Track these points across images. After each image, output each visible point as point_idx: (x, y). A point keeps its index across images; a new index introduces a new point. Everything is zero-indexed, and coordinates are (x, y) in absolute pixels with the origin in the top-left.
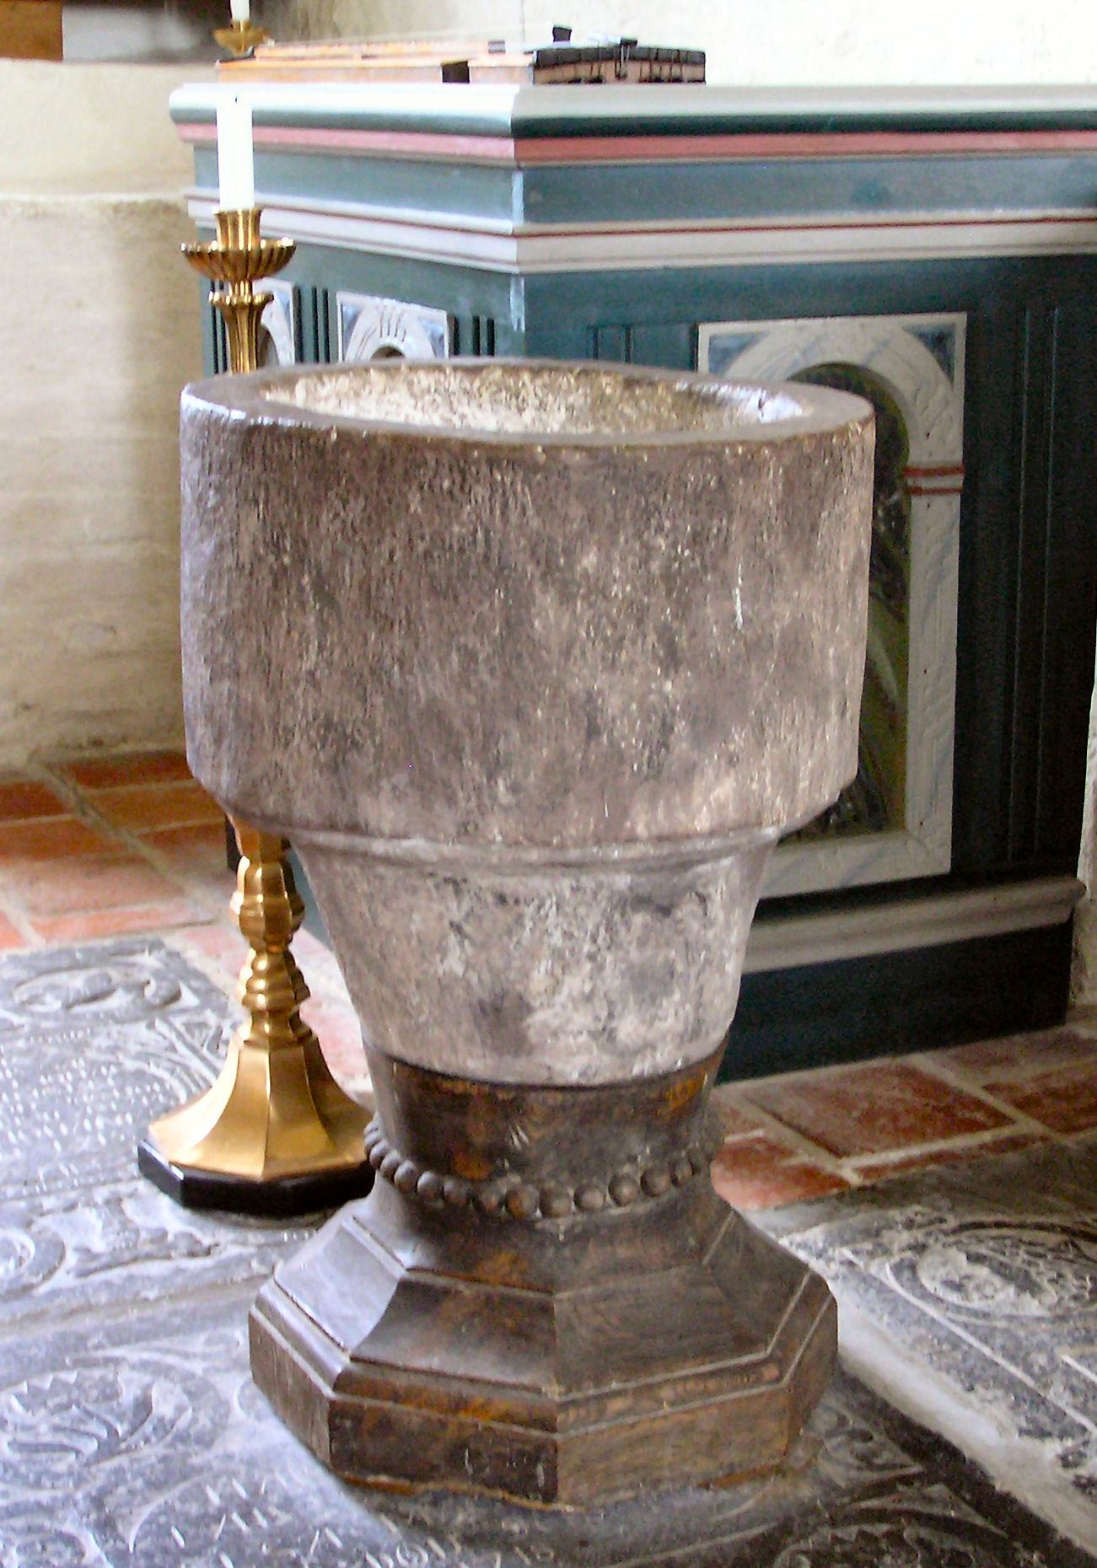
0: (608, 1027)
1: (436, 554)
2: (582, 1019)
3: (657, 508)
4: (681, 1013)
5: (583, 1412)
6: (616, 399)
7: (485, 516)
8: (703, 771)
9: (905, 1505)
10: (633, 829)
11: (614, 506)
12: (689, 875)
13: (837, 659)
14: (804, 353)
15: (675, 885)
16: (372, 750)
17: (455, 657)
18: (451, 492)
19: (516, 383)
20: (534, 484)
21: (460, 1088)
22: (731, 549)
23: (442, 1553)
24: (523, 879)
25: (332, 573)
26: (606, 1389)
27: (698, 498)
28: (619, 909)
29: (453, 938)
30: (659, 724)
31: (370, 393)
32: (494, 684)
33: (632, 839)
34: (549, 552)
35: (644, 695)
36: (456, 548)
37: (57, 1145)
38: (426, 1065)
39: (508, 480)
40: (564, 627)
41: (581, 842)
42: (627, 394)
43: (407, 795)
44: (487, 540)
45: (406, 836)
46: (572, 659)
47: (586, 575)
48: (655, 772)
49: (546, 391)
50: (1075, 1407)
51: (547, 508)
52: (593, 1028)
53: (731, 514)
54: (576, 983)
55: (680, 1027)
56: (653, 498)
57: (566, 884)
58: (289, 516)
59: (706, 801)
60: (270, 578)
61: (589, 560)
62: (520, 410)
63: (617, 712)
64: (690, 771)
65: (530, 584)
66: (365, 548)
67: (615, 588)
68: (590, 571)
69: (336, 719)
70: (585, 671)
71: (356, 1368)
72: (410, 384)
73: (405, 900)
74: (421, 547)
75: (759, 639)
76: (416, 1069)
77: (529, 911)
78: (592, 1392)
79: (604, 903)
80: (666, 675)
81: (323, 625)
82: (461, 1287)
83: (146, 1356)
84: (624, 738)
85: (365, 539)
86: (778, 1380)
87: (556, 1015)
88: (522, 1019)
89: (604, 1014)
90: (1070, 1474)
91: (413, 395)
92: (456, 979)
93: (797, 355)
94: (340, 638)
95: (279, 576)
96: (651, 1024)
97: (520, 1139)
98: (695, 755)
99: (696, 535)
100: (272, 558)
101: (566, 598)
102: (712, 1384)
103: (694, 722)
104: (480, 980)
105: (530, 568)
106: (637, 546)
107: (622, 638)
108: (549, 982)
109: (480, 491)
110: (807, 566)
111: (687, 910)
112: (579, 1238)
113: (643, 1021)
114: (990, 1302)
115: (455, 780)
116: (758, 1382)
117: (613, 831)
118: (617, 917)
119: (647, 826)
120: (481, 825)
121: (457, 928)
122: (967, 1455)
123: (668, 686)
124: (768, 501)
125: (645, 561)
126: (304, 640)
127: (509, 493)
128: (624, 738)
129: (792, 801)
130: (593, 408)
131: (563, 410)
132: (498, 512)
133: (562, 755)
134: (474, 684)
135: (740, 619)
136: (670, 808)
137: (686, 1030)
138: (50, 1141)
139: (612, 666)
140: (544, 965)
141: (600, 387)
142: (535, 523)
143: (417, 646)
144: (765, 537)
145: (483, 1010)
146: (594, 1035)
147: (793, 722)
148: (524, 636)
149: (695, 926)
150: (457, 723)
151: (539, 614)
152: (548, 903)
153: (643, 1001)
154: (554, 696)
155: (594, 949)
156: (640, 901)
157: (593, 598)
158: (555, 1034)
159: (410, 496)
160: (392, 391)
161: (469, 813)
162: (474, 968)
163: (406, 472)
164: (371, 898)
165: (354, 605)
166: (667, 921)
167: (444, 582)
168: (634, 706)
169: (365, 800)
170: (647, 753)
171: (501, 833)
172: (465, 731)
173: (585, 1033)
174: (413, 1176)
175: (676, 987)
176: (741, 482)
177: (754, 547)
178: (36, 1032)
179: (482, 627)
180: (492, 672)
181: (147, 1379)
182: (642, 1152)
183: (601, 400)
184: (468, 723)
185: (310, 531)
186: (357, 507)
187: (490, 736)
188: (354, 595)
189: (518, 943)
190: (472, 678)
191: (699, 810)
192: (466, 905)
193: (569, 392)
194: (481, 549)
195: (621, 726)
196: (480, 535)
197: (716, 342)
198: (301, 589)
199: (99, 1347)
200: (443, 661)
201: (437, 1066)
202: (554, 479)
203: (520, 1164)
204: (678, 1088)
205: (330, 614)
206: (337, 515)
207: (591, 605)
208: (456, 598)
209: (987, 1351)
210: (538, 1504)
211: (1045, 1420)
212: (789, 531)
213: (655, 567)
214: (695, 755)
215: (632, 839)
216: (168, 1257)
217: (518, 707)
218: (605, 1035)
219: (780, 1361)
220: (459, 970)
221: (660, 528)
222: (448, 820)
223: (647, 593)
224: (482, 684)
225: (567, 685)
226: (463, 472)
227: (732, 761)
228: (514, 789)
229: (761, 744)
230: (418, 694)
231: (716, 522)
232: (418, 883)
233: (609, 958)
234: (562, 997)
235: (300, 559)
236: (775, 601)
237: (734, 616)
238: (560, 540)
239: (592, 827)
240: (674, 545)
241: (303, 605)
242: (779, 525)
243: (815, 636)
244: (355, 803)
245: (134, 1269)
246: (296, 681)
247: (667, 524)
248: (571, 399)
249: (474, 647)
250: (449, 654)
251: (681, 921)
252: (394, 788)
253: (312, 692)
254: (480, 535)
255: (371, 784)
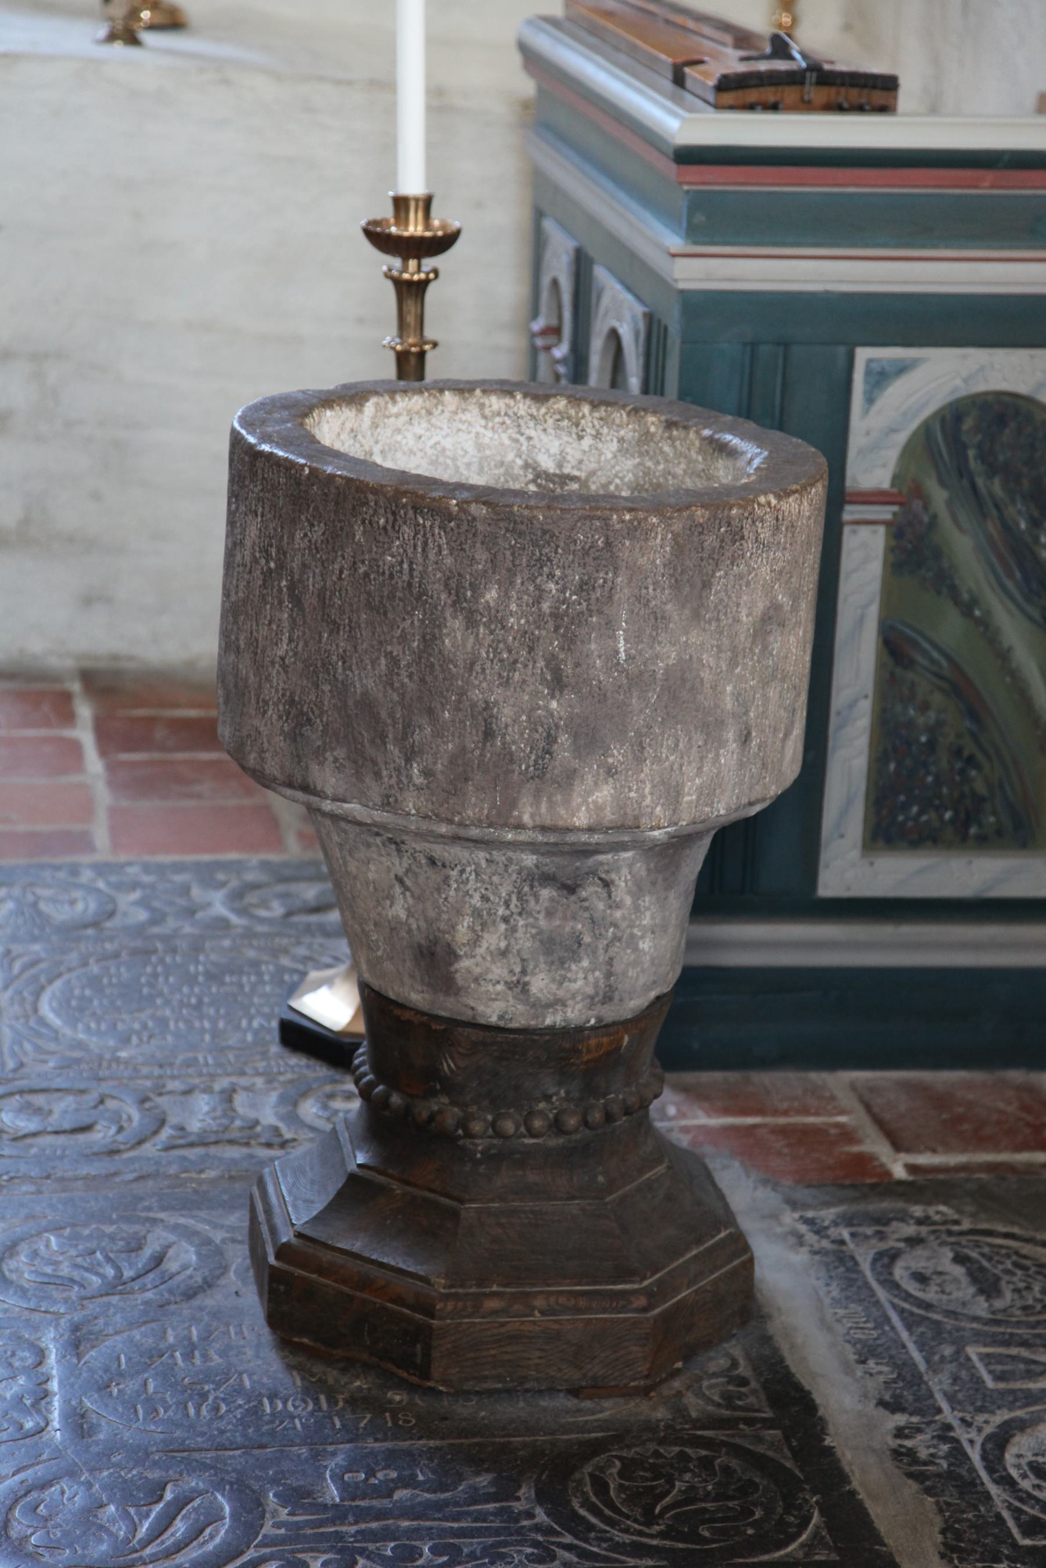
0: (522, 981)
1: (372, 576)
2: (498, 971)
3: (549, 560)
4: (591, 978)
5: (460, 1304)
6: (657, 438)
7: (410, 551)
8: (583, 776)
9: (738, 1441)
10: (520, 817)
11: (513, 554)
12: (591, 861)
13: (737, 696)
14: (966, 381)
15: (577, 868)
16: (321, 728)
17: (383, 661)
18: (385, 528)
19: (577, 413)
20: (448, 530)
21: (407, 1015)
22: (617, 597)
23: (324, 1406)
24: (447, 847)
25: (300, 581)
26: (487, 1290)
27: (586, 553)
28: (528, 883)
29: (398, 889)
30: (544, 734)
31: (443, 411)
32: (411, 686)
33: (519, 826)
34: (459, 587)
35: (533, 710)
36: (387, 573)
37: (207, 1038)
38: (383, 992)
39: (428, 524)
40: (469, 646)
41: (478, 823)
42: (666, 435)
43: (345, 767)
44: (411, 570)
45: (345, 801)
46: (474, 674)
47: (488, 607)
48: (540, 774)
49: (602, 423)
50: (945, 1394)
51: (458, 548)
52: (509, 979)
53: (616, 569)
54: (493, 939)
55: (590, 990)
56: (546, 550)
57: (481, 855)
58: (275, 529)
59: (585, 801)
60: (261, 577)
61: (491, 595)
62: (580, 438)
63: (509, 721)
64: (571, 775)
65: (442, 611)
66: (323, 563)
67: (512, 620)
68: (492, 604)
69: (297, 698)
70: (484, 685)
71: (294, 1241)
72: (482, 406)
73: (362, 853)
74: (362, 569)
75: (641, 673)
76: (378, 994)
77: (454, 874)
78: (473, 1290)
79: (514, 876)
80: (553, 697)
81: (293, 621)
82: (395, 1185)
83: (182, 1221)
84: (514, 742)
85: (324, 557)
86: (645, 1310)
87: (477, 965)
88: (451, 964)
89: (518, 969)
90: (894, 1443)
91: (484, 417)
92: (401, 923)
93: (958, 382)
94: (304, 633)
95: (268, 574)
96: (561, 984)
97: (449, 1066)
98: (576, 764)
99: (583, 584)
100: (263, 561)
101: (471, 623)
102: (582, 1303)
103: (576, 736)
104: (419, 928)
105: (443, 596)
106: (531, 588)
107: (515, 662)
108: (471, 935)
109: (407, 531)
110: (696, 615)
111: (591, 890)
112: (495, 1159)
113: (553, 980)
114: (945, 1297)
115: (380, 760)
116: (623, 1309)
117: (503, 817)
118: (526, 889)
119: (532, 816)
120: (400, 799)
121: (400, 880)
122: (821, 1412)
123: (554, 704)
124: (654, 561)
125: (537, 601)
126: (279, 632)
127: (428, 535)
128: (514, 742)
129: (674, 811)
130: (639, 442)
131: (615, 440)
132: (420, 550)
133: (463, 750)
134: (396, 685)
135: (623, 656)
136: (552, 805)
137: (597, 994)
138: (203, 1030)
139: (506, 683)
140: (467, 921)
141: (645, 424)
142: (449, 561)
143: (355, 648)
144: (651, 590)
145: (421, 952)
146: (510, 986)
147: (677, 745)
148: (437, 650)
149: (601, 906)
150: (384, 714)
151: (449, 635)
152: (468, 869)
153: (552, 963)
154: (459, 701)
155: (508, 913)
156: (548, 879)
157: (493, 627)
158: (476, 980)
159: (356, 527)
160: (464, 411)
161: (391, 787)
162: (413, 916)
163: (354, 508)
164: (341, 846)
165: (315, 609)
166: (573, 898)
167: (377, 599)
168: (524, 718)
169: (314, 767)
170: (533, 757)
171: (414, 807)
172: (389, 721)
173: (502, 983)
174: (371, 1085)
175: (582, 954)
176: (627, 543)
177: (638, 599)
178: (249, 934)
179: (403, 639)
180: (410, 676)
181: (172, 1238)
182: (557, 1094)
183: (646, 437)
184: (392, 715)
185: (288, 543)
186: (319, 530)
187: (408, 728)
188: (315, 601)
189: (446, 899)
190: (395, 678)
191: (578, 810)
192: (406, 862)
193: (620, 426)
194: (406, 578)
195: (513, 733)
196: (405, 566)
197: (873, 365)
198: (280, 590)
199: (149, 1209)
200: (374, 662)
201: (392, 995)
202: (464, 527)
203: (449, 1087)
204: (593, 1042)
205: (298, 615)
206: (306, 535)
207: (492, 632)
208: (385, 614)
209: (904, 1335)
210: (414, 1379)
211: (908, 1396)
212: (676, 586)
213: (546, 606)
214: (576, 764)
215: (519, 826)
216: (247, 1144)
217: (430, 708)
218: (520, 987)
219: (654, 1296)
220: (403, 915)
221: (551, 576)
222: (375, 792)
223: (538, 628)
224: (403, 685)
225: (469, 694)
226: (394, 513)
227: (611, 772)
228: (427, 773)
229: (640, 760)
230: (355, 687)
231: (602, 575)
232: (371, 840)
233: (521, 923)
234: (480, 951)
235: (281, 566)
236: (660, 643)
237: (617, 652)
238: (468, 577)
239: (486, 812)
240: (563, 591)
241: (281, 602)
242: (666, 582)
243: (705, 675)
244: (307, 767)
245: (213, 1150)
246: (273, 663)
247: (558, 573)
248: (622, 433)
249: (398, 655)
250: (378, 658)
251: (584, 900)
252: (336, 760)
253: (283, 676)
254: (405, 566)
255: (319, 754)
